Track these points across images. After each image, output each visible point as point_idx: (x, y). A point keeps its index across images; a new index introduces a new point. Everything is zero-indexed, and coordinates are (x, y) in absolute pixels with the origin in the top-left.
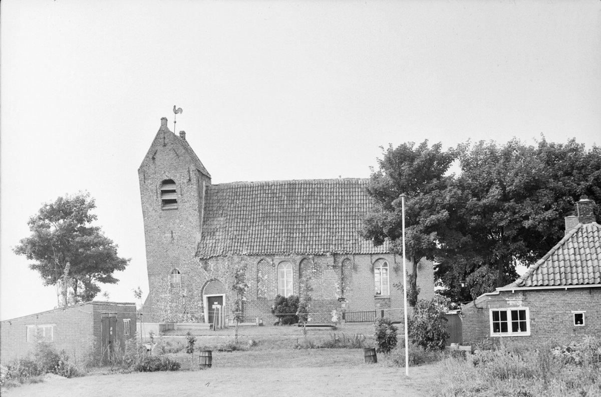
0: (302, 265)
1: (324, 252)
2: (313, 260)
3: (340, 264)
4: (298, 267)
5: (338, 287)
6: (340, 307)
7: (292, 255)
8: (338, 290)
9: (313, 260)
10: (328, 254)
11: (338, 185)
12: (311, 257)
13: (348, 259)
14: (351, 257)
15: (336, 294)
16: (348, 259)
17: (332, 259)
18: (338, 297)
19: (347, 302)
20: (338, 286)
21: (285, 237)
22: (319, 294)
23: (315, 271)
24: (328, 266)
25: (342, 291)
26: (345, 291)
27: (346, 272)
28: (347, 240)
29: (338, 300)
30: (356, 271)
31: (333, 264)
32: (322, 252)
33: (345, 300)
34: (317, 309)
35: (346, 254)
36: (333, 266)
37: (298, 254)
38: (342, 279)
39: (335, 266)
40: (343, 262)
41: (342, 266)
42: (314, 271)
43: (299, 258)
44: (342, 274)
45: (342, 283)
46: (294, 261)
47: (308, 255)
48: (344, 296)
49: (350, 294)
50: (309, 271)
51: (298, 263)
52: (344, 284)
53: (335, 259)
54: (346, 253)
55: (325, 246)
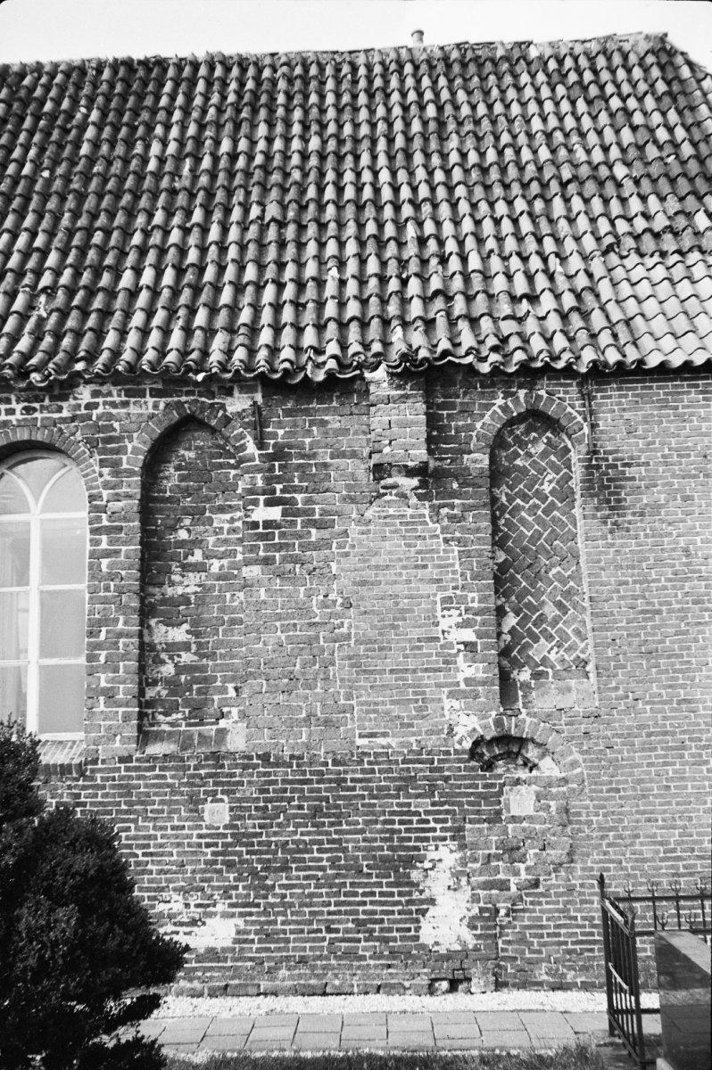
0: (171, 478)
1: (342, 366)
2: (259, 425)
3: (478, 461)
4: (133, 485)
5: (469, 646)
6: (495, 818)
7: (85, 394)
8: (467, 670)
9: (259, 425)
10: (381, 373)
11: (408, 69)
12: (238, 403)
13: (538, 419)
14: (565, 401)
15: (447, 703)
16: (538, 419)
17: (414, 412)
18: (469, 724)
19: (548, 768)
20: (469, 635)
21: (51, 291)
22: (308, 701)
23: (275, 513)
24: (379, 471)
25: (506, 681)
26: (524, 676)
27: (527, 524)
28: (515, 300)
29: (473, 753)
30: (617, 507)
31: (420, 454)
32: (332, 364)
33: (532, 753)
34: (295, 834)
35: (530, 374)
36: (421, 471)
37: (131, 380)
38: (502, 579)
39: (440, 475)
40: (497, 444)
41: (496, 474)
42: (262, 513)
43: (149, 410)
44: (499, 541)
45: (500, 612)
46: (105, 442)
47: (221, 385)
48: (524, 723)
49: (578, 695)
50: (221, 520)
51: (134, 453)
52: (511, 621)
53: (432, 421)
54: (525, 367)
55: (354, 329)
